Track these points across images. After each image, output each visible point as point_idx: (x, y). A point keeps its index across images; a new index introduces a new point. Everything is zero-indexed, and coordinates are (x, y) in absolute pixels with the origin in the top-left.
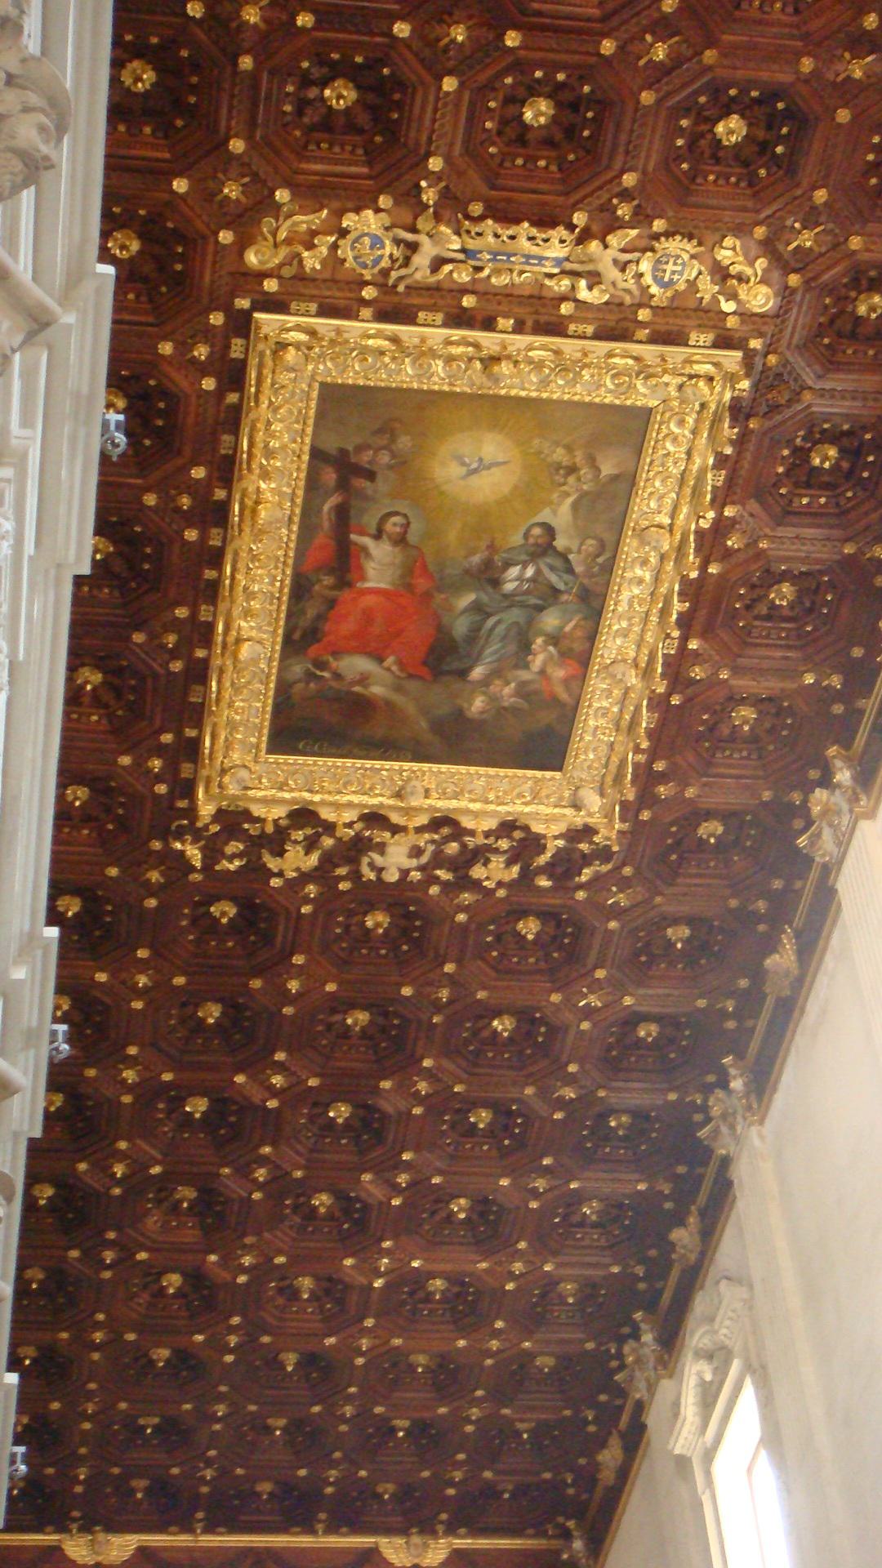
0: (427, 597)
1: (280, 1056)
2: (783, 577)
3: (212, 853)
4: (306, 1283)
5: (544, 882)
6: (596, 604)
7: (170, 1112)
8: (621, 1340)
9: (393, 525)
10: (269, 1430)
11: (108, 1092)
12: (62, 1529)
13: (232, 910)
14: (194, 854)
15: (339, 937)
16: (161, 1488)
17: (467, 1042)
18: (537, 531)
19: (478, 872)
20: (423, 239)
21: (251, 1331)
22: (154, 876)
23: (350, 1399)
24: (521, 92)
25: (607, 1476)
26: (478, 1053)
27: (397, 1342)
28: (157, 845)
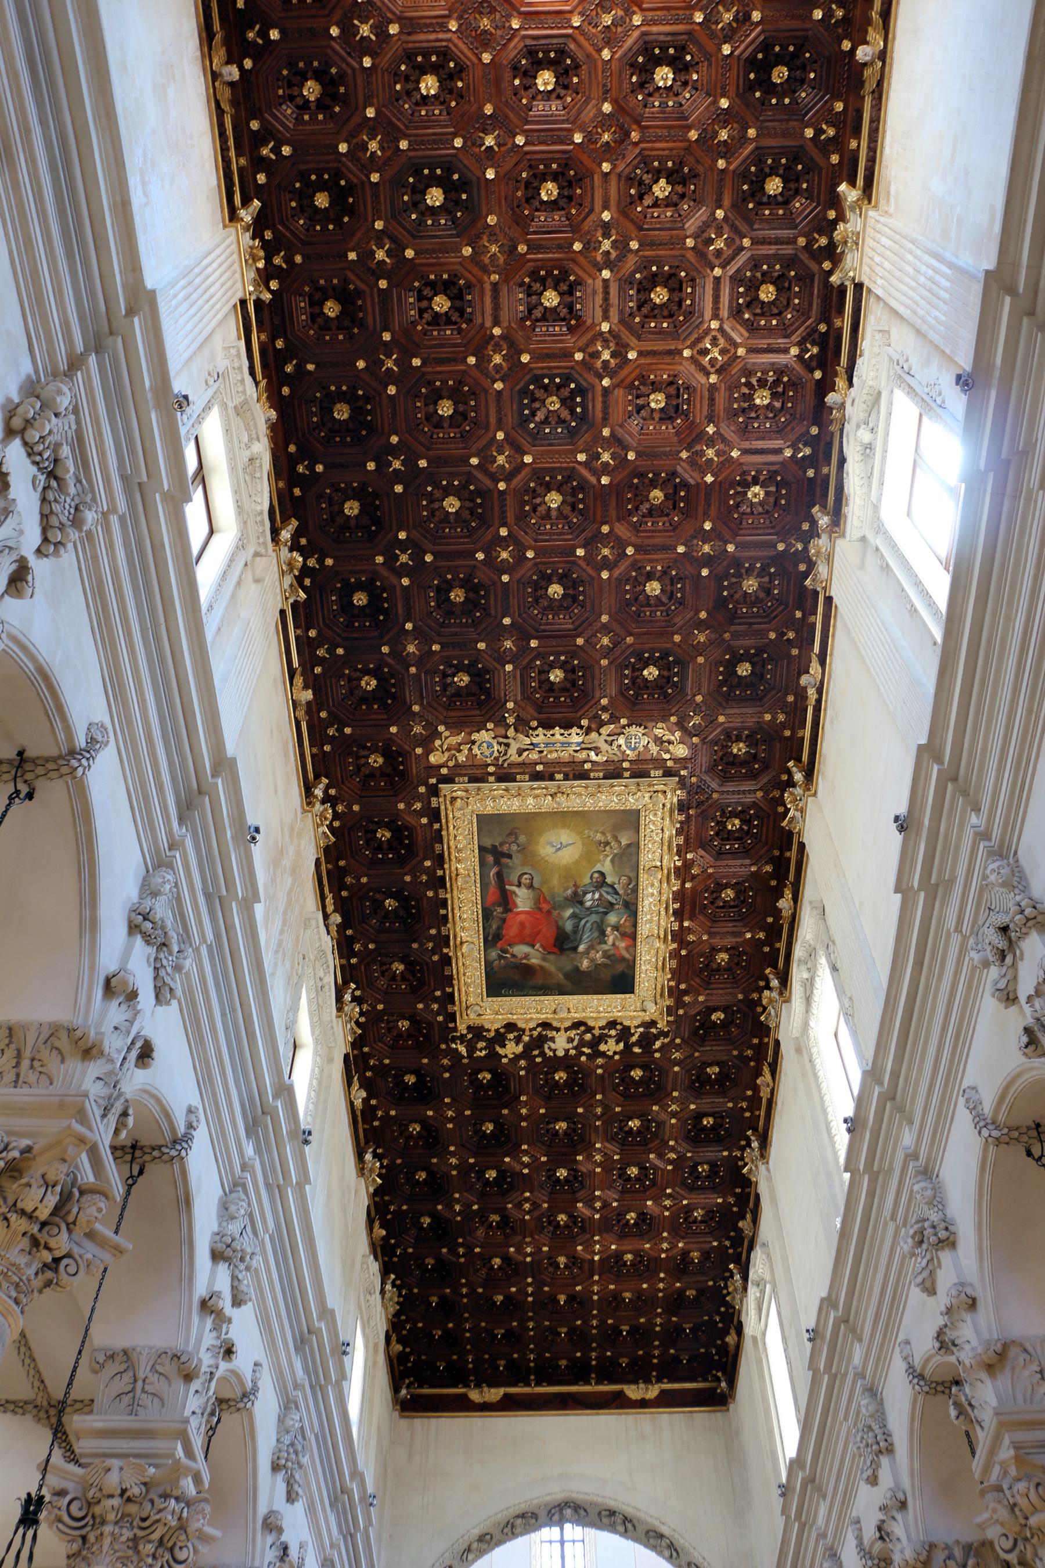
0: (549, 912)
1: (525, 1147)
2: (727, 886)
3: (471, 1049)
4: (562, 1260)
5: (637, 1050)
6: (633, 908)
7: (478, 1179)
8: (726, 1279)
9: (525, 879)
11: (444, 1169)
13: (488, 1076)
14: (462, 1049)
15: (543, 1086)
16: (511, 1364)
17: (617, 1134)
18: (596, 875)
19: (603, 1047)
20: (511, 741)
21: (539, 1284)
22: (445, 1062)
23: (594, 1317)
24: (546, 668)
25: (732, 1349)
26: (625, 1139)
27: (612, 1287)
28: (443, 1046)
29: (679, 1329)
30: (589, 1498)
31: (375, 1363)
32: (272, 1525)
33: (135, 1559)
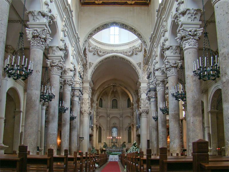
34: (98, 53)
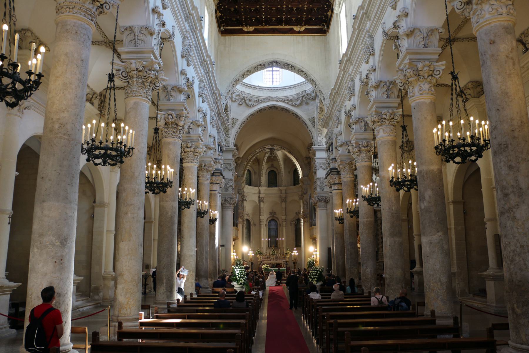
10: (273, 10)
12: (242, 26)
16: (257, 19)
23: (284, 4)
25: (329, 16)
29: (312, 9)
30: (281, 60)
31: (212, 20)
32: (183, 73)
33: (144, 87)
34: (246, 103)
